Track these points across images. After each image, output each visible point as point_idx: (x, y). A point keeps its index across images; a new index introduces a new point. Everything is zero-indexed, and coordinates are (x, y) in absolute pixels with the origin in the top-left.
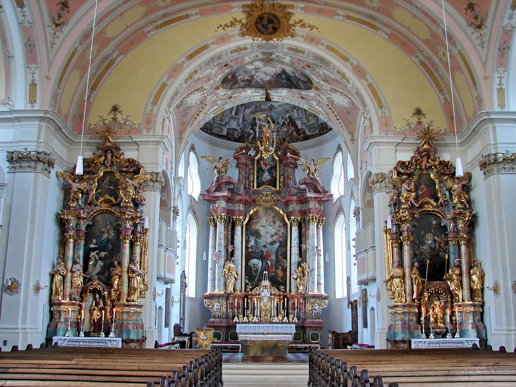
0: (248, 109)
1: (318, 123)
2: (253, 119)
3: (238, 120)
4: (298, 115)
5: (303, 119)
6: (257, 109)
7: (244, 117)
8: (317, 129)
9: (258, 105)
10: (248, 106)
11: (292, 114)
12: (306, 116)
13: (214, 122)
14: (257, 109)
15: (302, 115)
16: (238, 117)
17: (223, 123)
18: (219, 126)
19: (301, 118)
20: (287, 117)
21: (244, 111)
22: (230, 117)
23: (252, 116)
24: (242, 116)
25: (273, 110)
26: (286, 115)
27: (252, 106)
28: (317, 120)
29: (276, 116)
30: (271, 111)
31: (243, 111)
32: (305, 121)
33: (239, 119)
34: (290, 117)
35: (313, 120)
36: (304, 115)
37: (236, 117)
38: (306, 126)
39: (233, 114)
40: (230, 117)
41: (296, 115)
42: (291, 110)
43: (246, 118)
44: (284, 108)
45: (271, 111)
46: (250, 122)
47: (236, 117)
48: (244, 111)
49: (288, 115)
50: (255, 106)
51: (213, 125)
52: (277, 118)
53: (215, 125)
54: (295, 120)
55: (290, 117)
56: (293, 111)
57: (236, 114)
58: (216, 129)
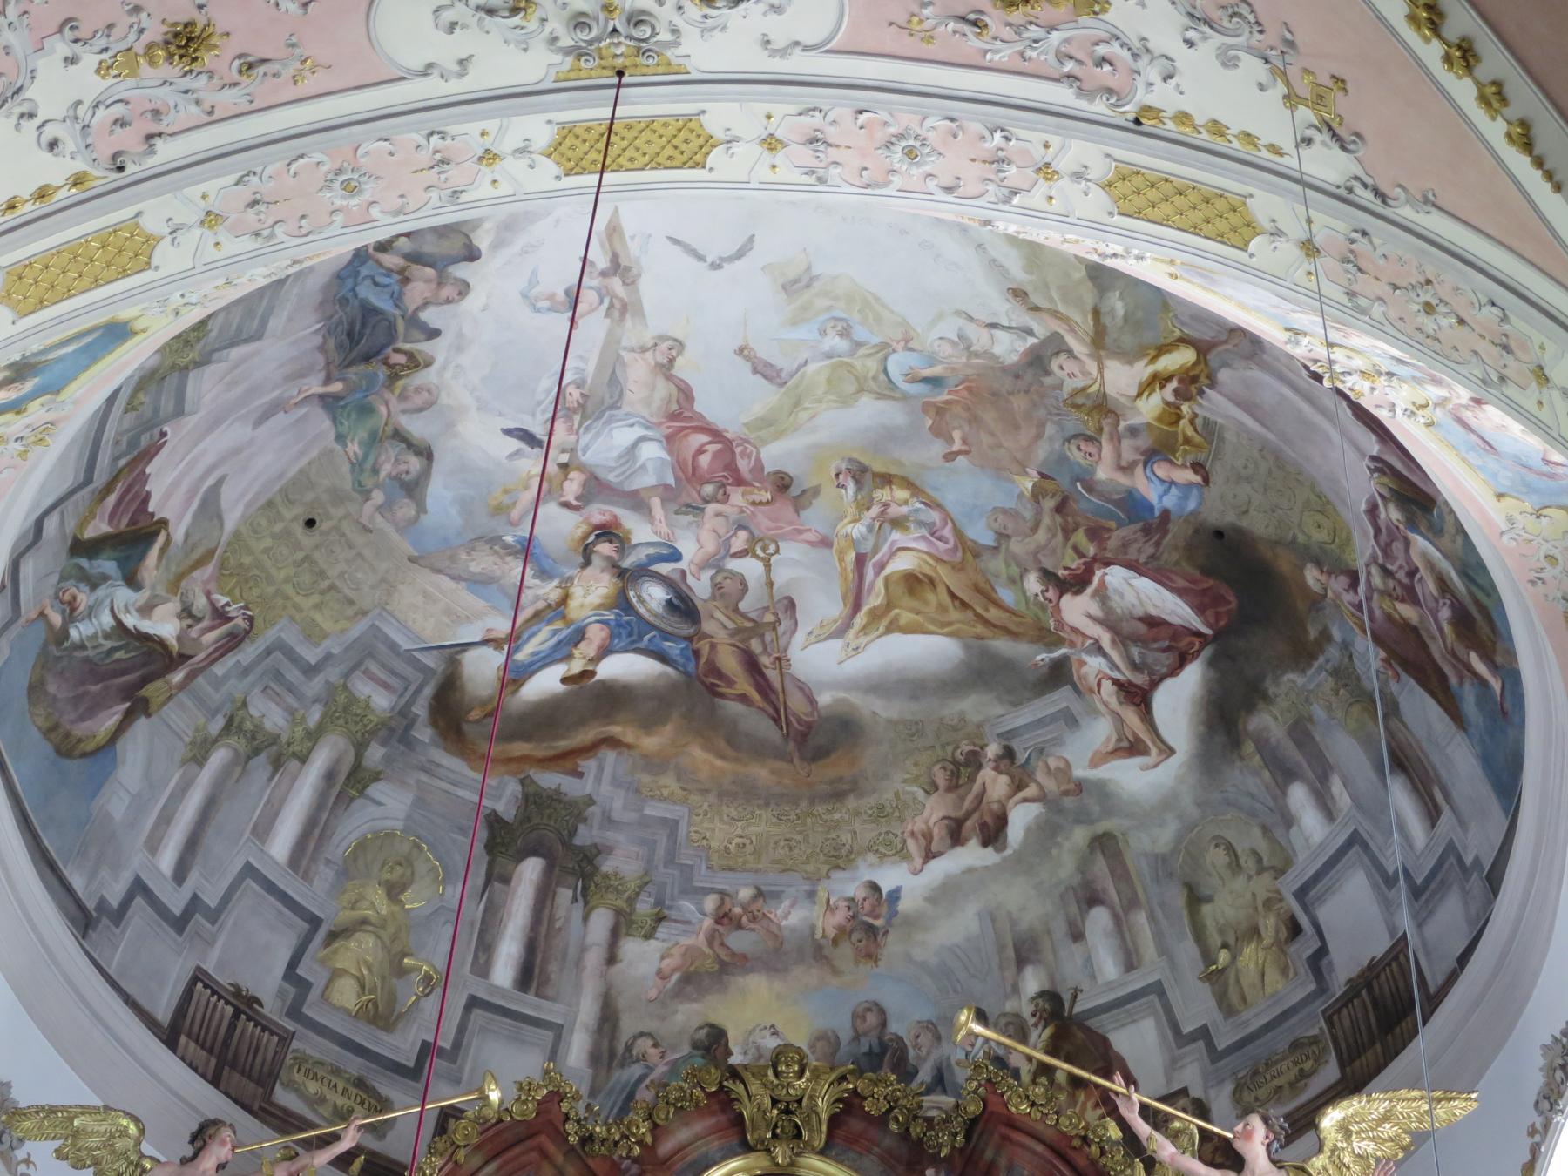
0: (649, 936)
1: (1322, 988)
2: (695, 1045)
3: (549, 1036)
4: (1130, 963)
5: (1174, 995)
6: (739, 941)
7: (608, 1018)
8: (1319, 1060)
9: (745, 893)
10: (644, 907)
11: (1071, 971)
12: (1208, 957)
13: (295, 1012)
14: (739, 941)
15: (1163, 950)
16: (549, 1011)
17: (402, 1045)
18: (354, 1065)
19: (1158, 989)
20: (1026, 1010)
21: (612, 959)
22: (473, 1002)
23: (689, 1016)
24: (587, 1010)
25: (892, 946)
26: (1016, 990)
27: (687, 906)
28: (1318, 959)
29: (926, 1013)
30: (871, 957)
31: (594, 958)
32: (1197, 1007)
33: (558, 1031)
34: (1053, 1006)
35: (1272, 975)
36: (1187, 951)
37: (527, 1004)
38: (1215, 1055)
39: (504, 971)
40: (473, 1002)
41: (1109, 967)
42: (1060, 928)
43: (628, 1026)
44: (991, 916)
45: (871, 957)
46: (674, 1067)
47: (527, 1004)
48: (612, 959)
49: (1032, 982)
50: (710, 903)
51: (285, 1038)
52: (938, 1029)
53: (308, 1045)
54: (1093, 1023)
55: (1053, 1006)
56: (1077, 935)
57: (528, 976)
58: (313, 1087)
